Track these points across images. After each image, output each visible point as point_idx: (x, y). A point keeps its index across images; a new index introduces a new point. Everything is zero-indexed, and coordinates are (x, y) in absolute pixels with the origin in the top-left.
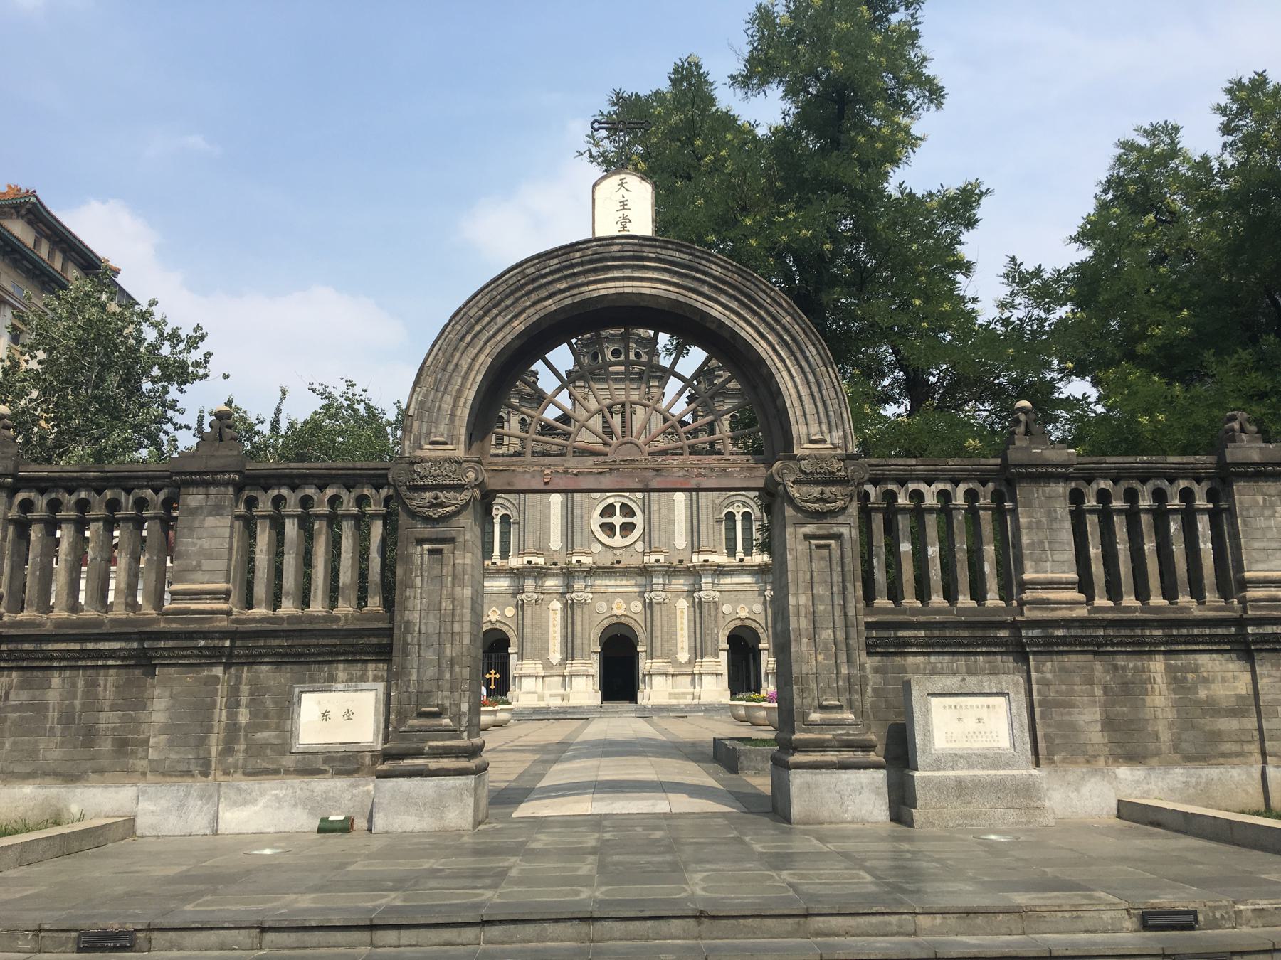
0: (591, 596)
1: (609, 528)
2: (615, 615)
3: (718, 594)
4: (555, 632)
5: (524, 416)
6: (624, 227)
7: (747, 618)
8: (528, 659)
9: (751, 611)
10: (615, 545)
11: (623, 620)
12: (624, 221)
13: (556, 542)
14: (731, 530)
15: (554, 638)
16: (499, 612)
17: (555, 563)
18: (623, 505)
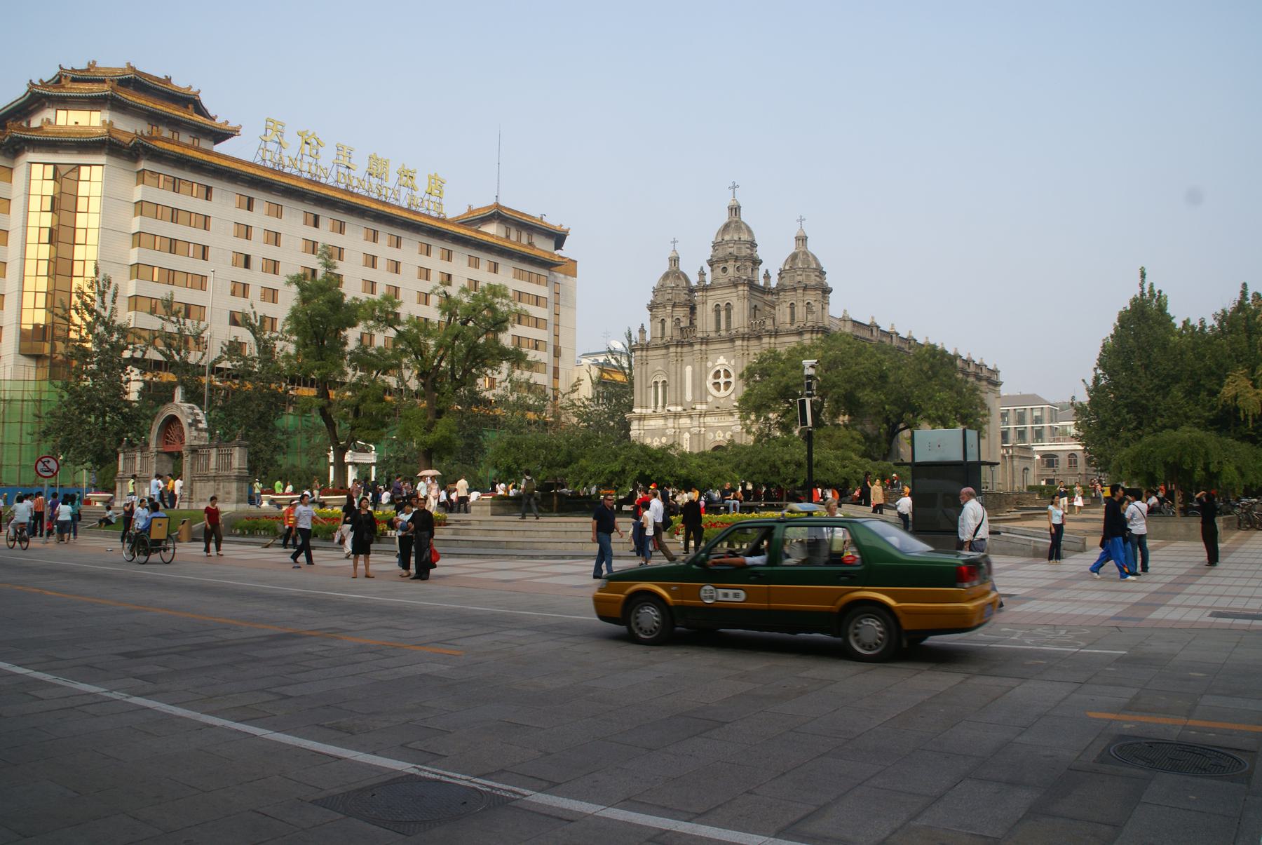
0: (703, 429)
1: (717, 385)
13: (689, 397)
18: (726, 370)
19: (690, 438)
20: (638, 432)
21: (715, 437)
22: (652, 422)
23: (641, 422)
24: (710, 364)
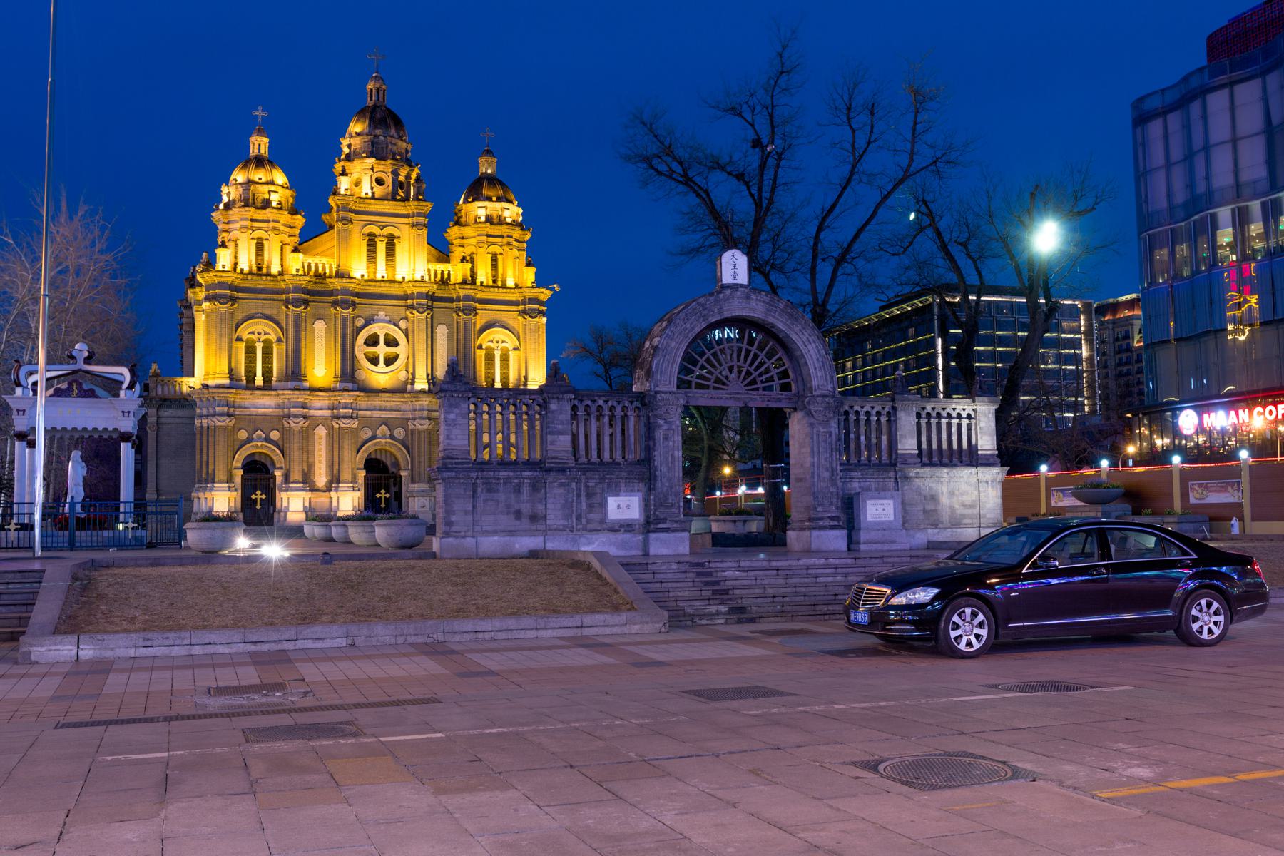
4: (320, 456)
6: (735, 279)
12: (735, 275)
18: (386, 335)
19: (328, 435)
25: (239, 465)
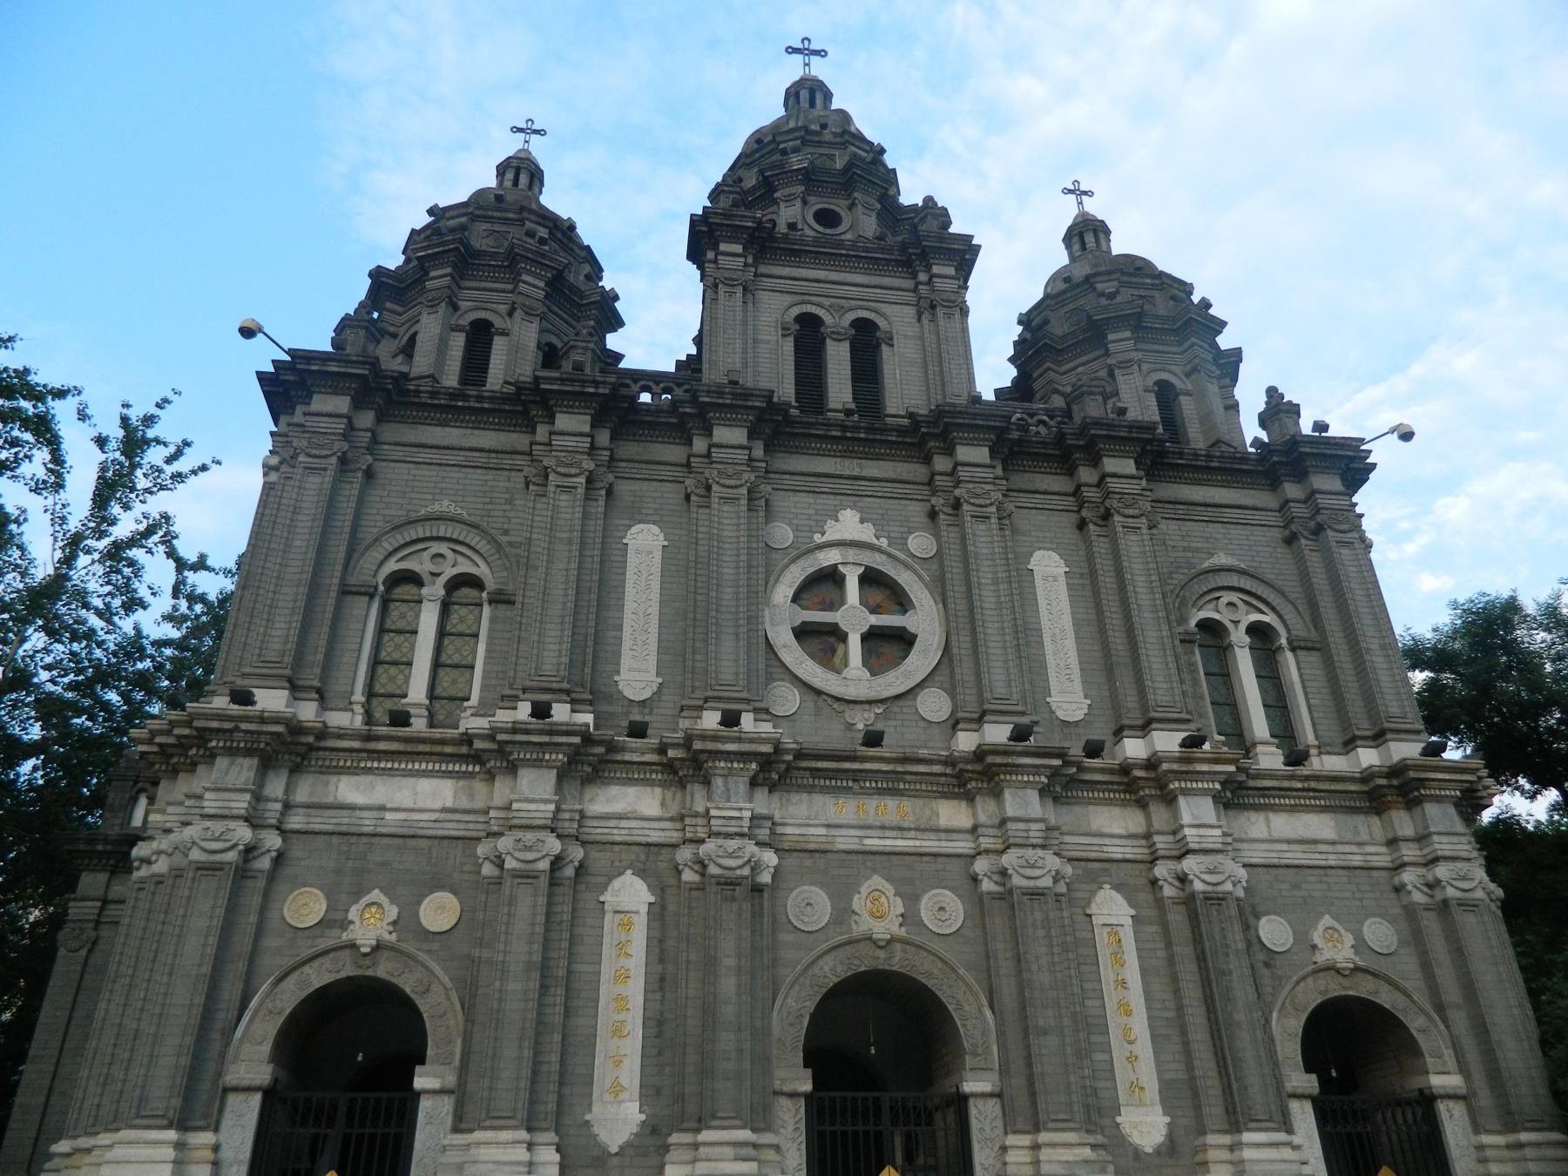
0: (770, 858)
2: (869, 939)
3: (1242, 874)
4: (621, 999)
5: (554, 340)
7: (1357, 969)
8: (494, 1120)
9: (1360, 945)
10: (850, 692)
11: (897, 962)
14: (1223, 675)
15: (618, 1031)
16: (393, 912)
17: (638, 731)
18: (870, 578)
19: (658, 913)
20: (244, 833)
21: (842, 914)
22: (350, 790)
23: (276, 786)
24: (783, 534)
25: (266, 1048)
